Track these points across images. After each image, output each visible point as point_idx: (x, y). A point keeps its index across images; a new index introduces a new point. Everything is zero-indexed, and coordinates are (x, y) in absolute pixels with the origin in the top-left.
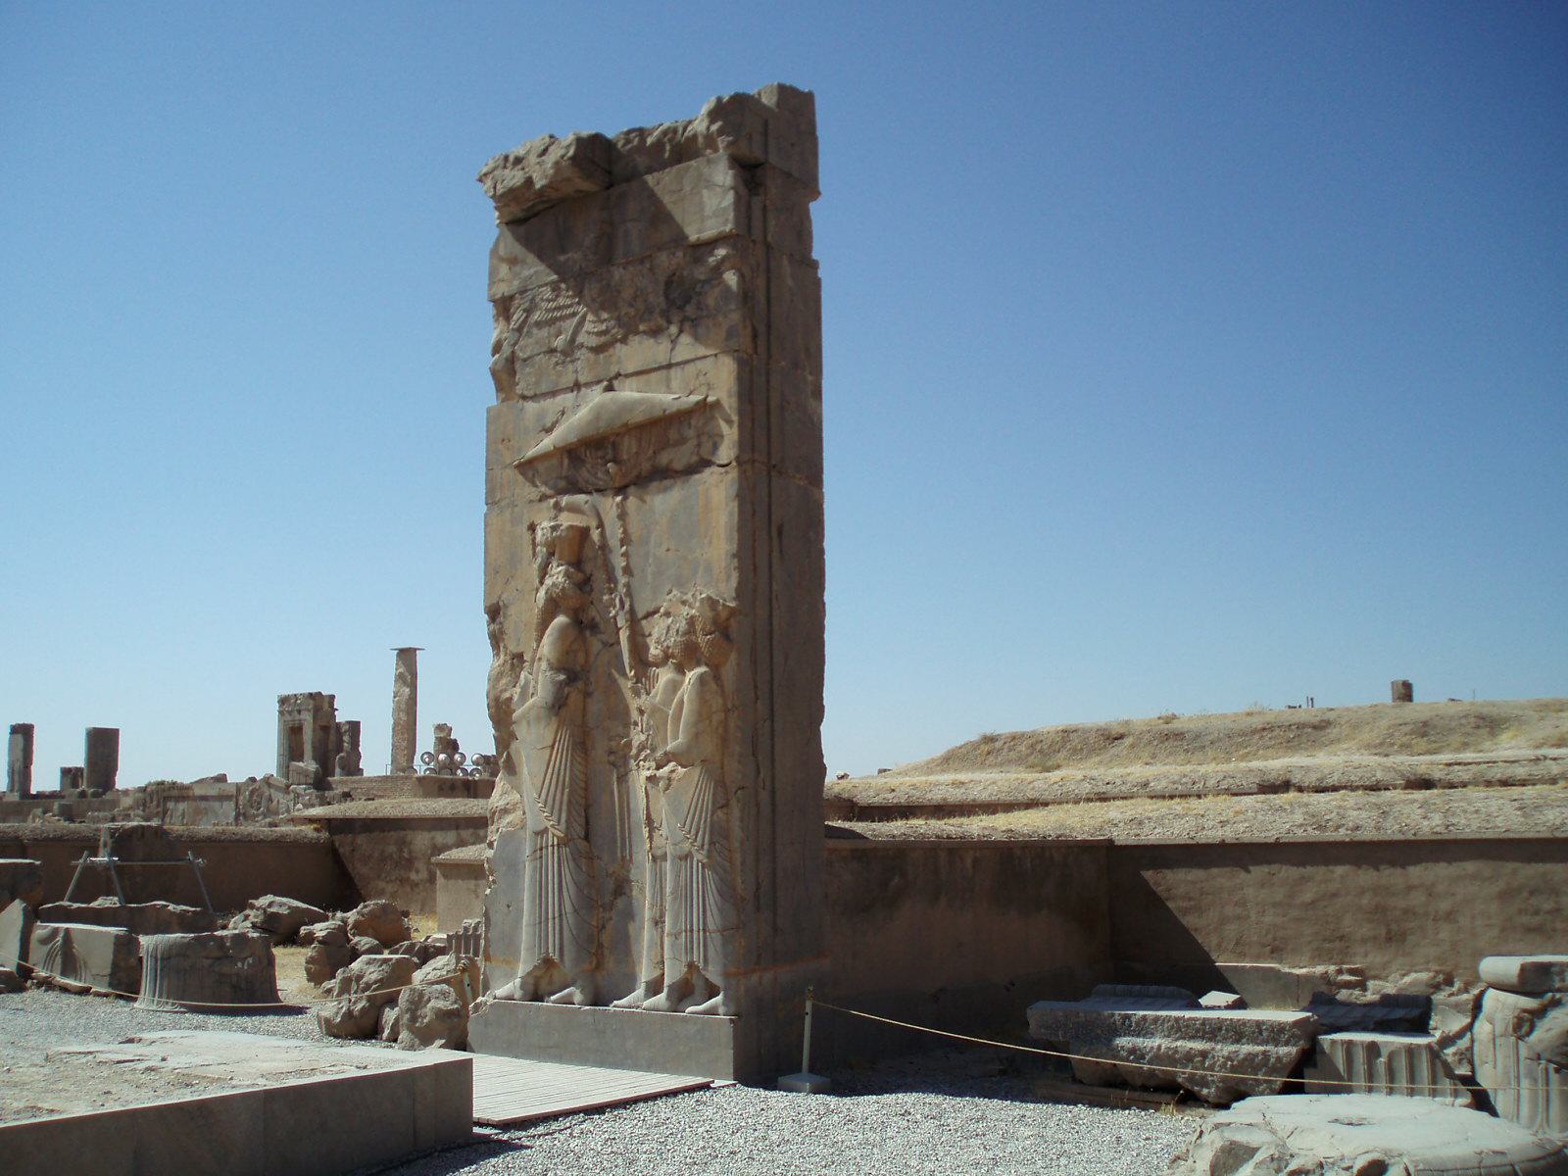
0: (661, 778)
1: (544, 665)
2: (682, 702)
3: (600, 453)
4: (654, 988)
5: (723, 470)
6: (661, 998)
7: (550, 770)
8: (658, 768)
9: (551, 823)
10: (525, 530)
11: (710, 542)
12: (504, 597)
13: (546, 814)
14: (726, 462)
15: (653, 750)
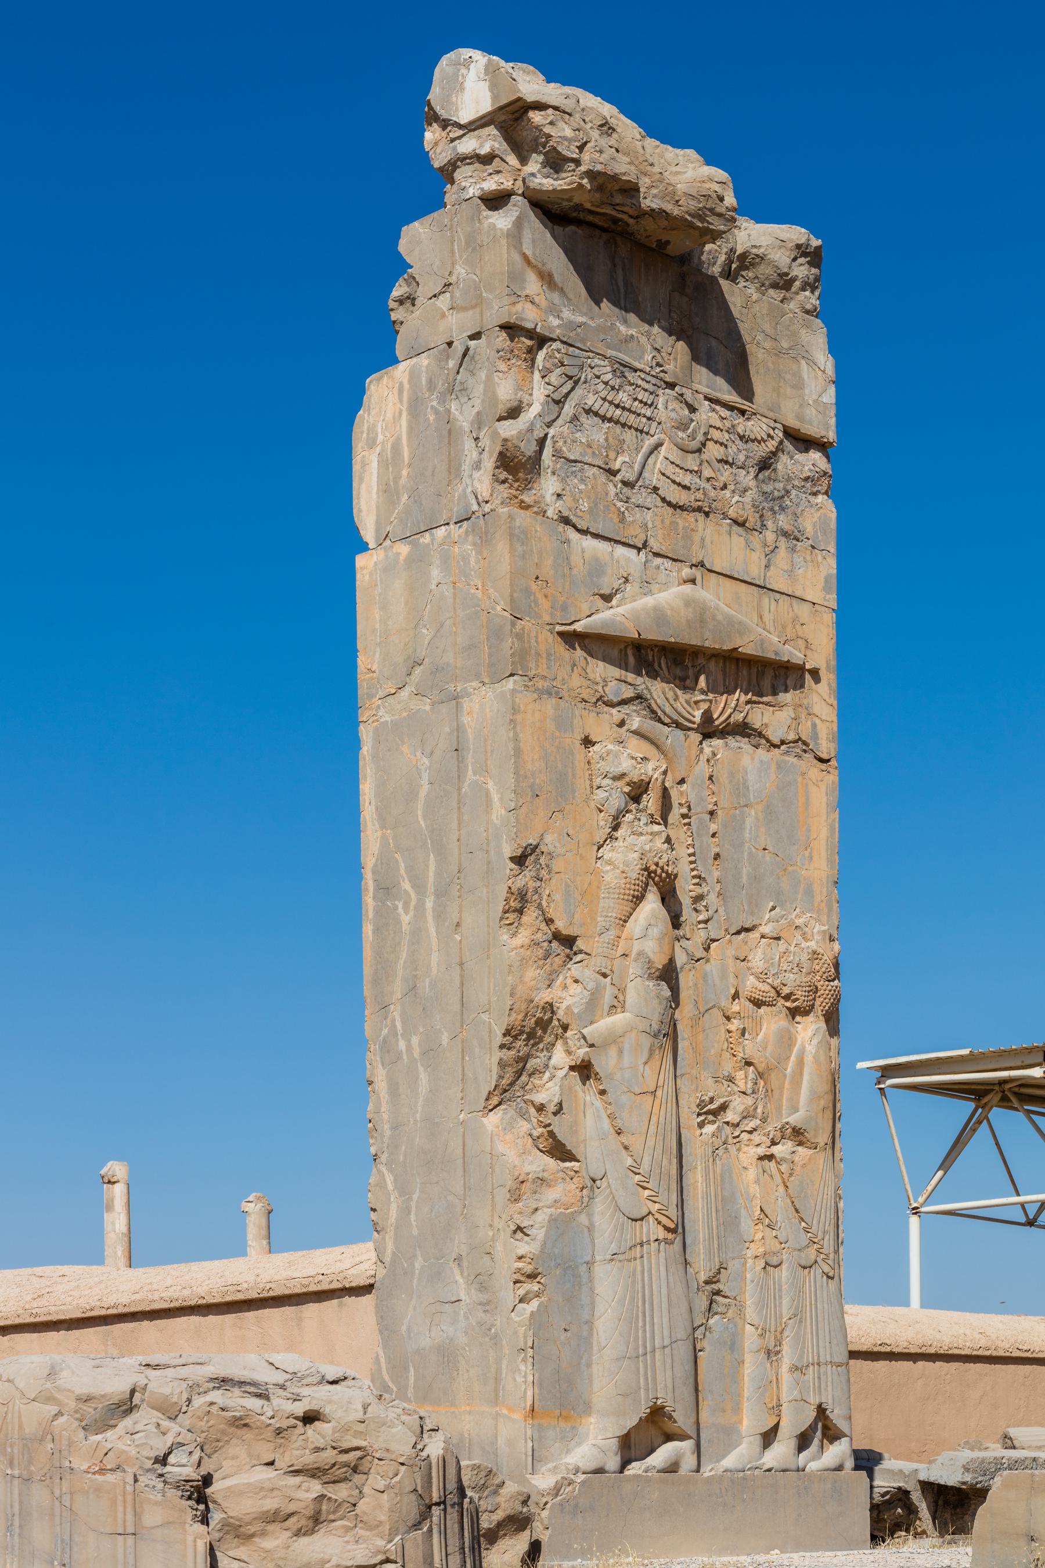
0: (783, 1159)
1: (634, 969)
2: (800, 1063)
3: (678, 672)
4: (769, 1437)
5: (823, 766)
6: (781, 1451)
7: (653, 1129)
8: (774, 1143)
9: (657, 1206)
10: (578, 743)
11: (811, 858)
12: (548, 838)
13: (647, 1193)
14: (825, 756)
15: (764, 1120)
